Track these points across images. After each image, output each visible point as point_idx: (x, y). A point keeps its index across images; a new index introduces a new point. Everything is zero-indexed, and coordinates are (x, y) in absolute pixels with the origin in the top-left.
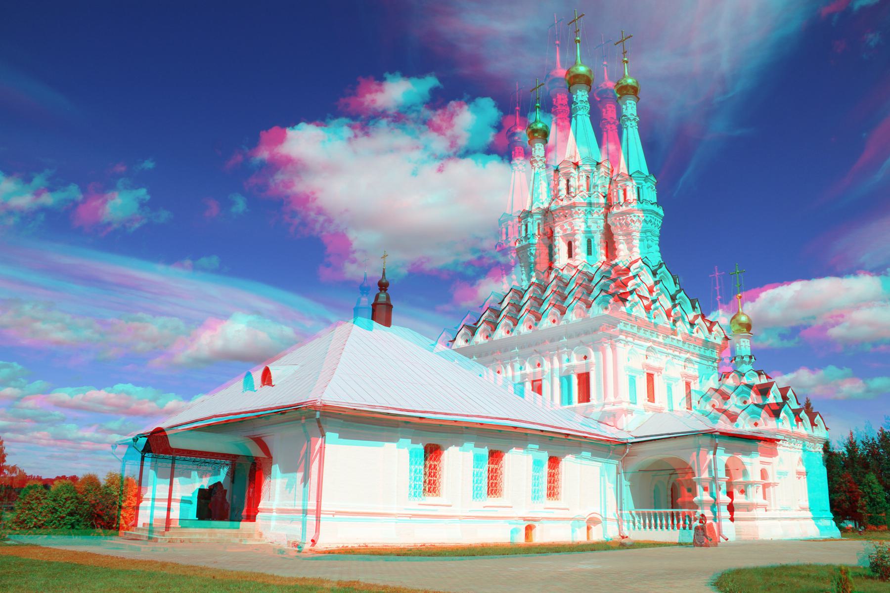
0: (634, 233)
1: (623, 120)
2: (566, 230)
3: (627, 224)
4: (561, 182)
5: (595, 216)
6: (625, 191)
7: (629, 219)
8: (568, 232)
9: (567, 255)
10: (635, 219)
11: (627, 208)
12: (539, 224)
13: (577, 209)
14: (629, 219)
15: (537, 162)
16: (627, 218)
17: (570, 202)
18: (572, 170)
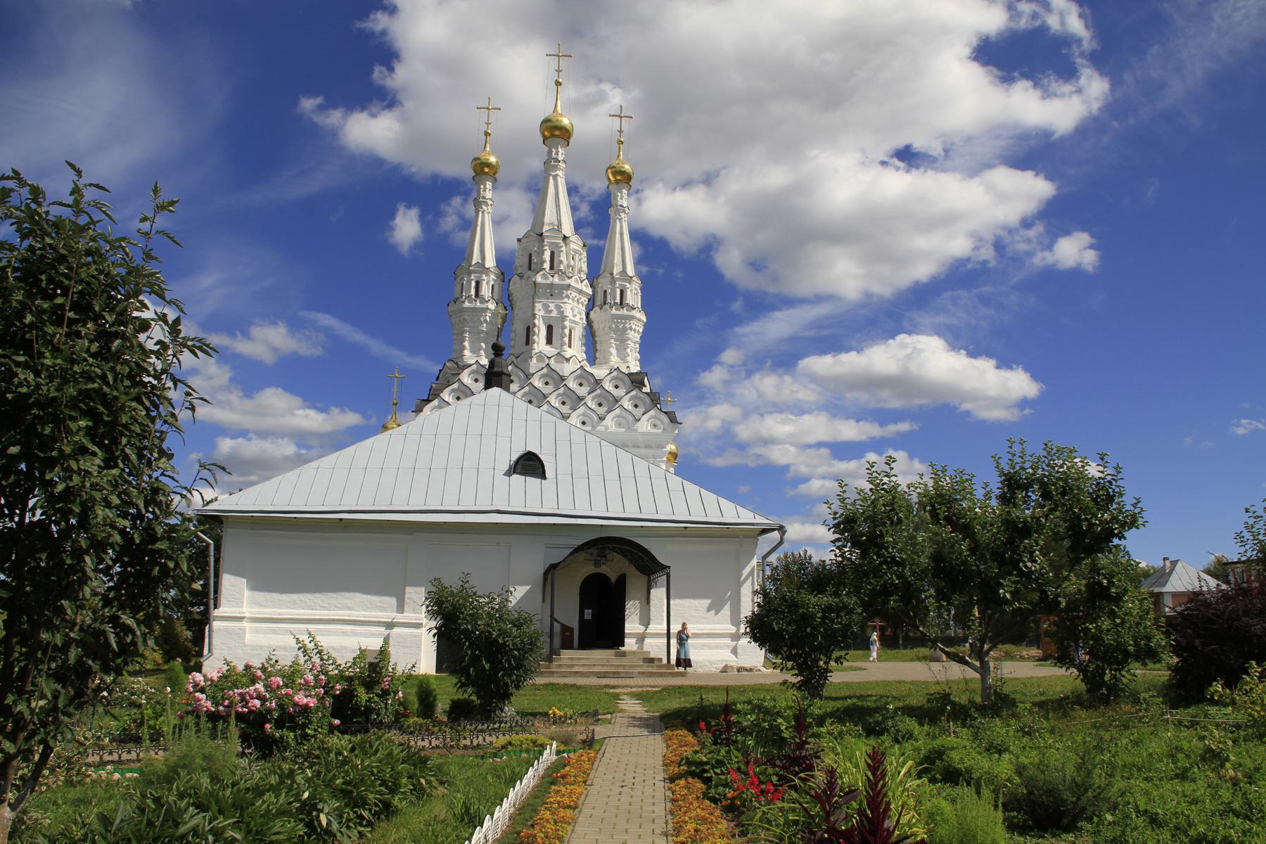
0: (629, 342)
1: (618, 209)
2: (551, 311)
3: (625, 329)
4: (546, 252)
5: (580, 306)
6: (622, 292)
7: (627, 326)
8: (554, 314)
9: (545, 341)
10: (633, 327)
11: (629, 313)
12: (493, 286)
13: (569, 292)
14: (627, 326)
15: (487, 205)
16: (626, 323)
17: (564, 283)
18: (562, 243)
